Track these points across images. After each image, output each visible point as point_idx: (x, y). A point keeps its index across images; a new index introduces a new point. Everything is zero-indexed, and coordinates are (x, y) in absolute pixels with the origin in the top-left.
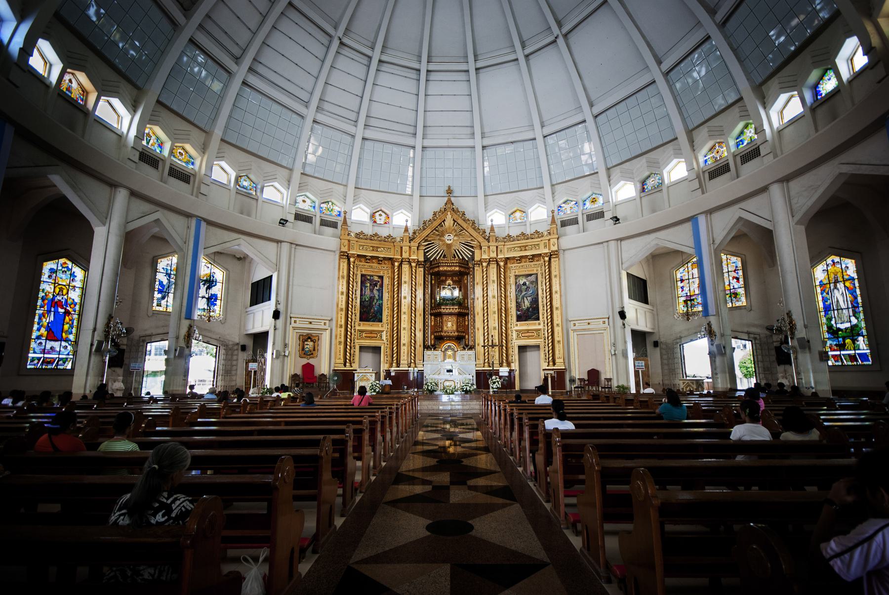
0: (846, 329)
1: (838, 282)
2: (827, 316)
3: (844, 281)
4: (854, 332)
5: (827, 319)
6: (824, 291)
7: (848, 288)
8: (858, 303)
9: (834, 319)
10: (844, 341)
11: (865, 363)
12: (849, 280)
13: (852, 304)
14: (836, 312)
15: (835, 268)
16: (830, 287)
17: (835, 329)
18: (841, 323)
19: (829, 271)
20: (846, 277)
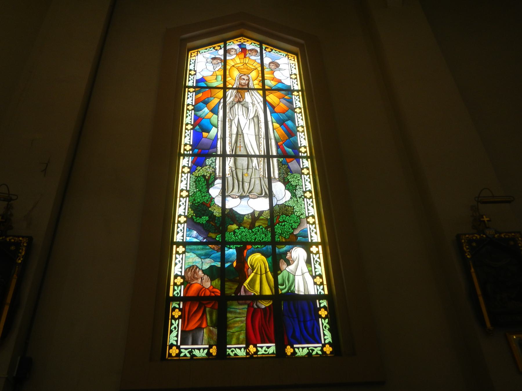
0: (255, 217)
1: (248, 89)
2: (200, 171)
3: (264, 89)
4: (278, 229)
5: (197, 181)
6: (206, 103)
7: (273, 107)
8: (295, 148)
9: (218, 183)
10: (242, 259)
11: (302, 350)
12: (279, 90)
13: (278, 147)
14: (230, 162)
15: (247, 60)
16: (225, 97)
17: (217, 213)
18: (241, 197)
19: (230, 63)
20: (269, 83)
